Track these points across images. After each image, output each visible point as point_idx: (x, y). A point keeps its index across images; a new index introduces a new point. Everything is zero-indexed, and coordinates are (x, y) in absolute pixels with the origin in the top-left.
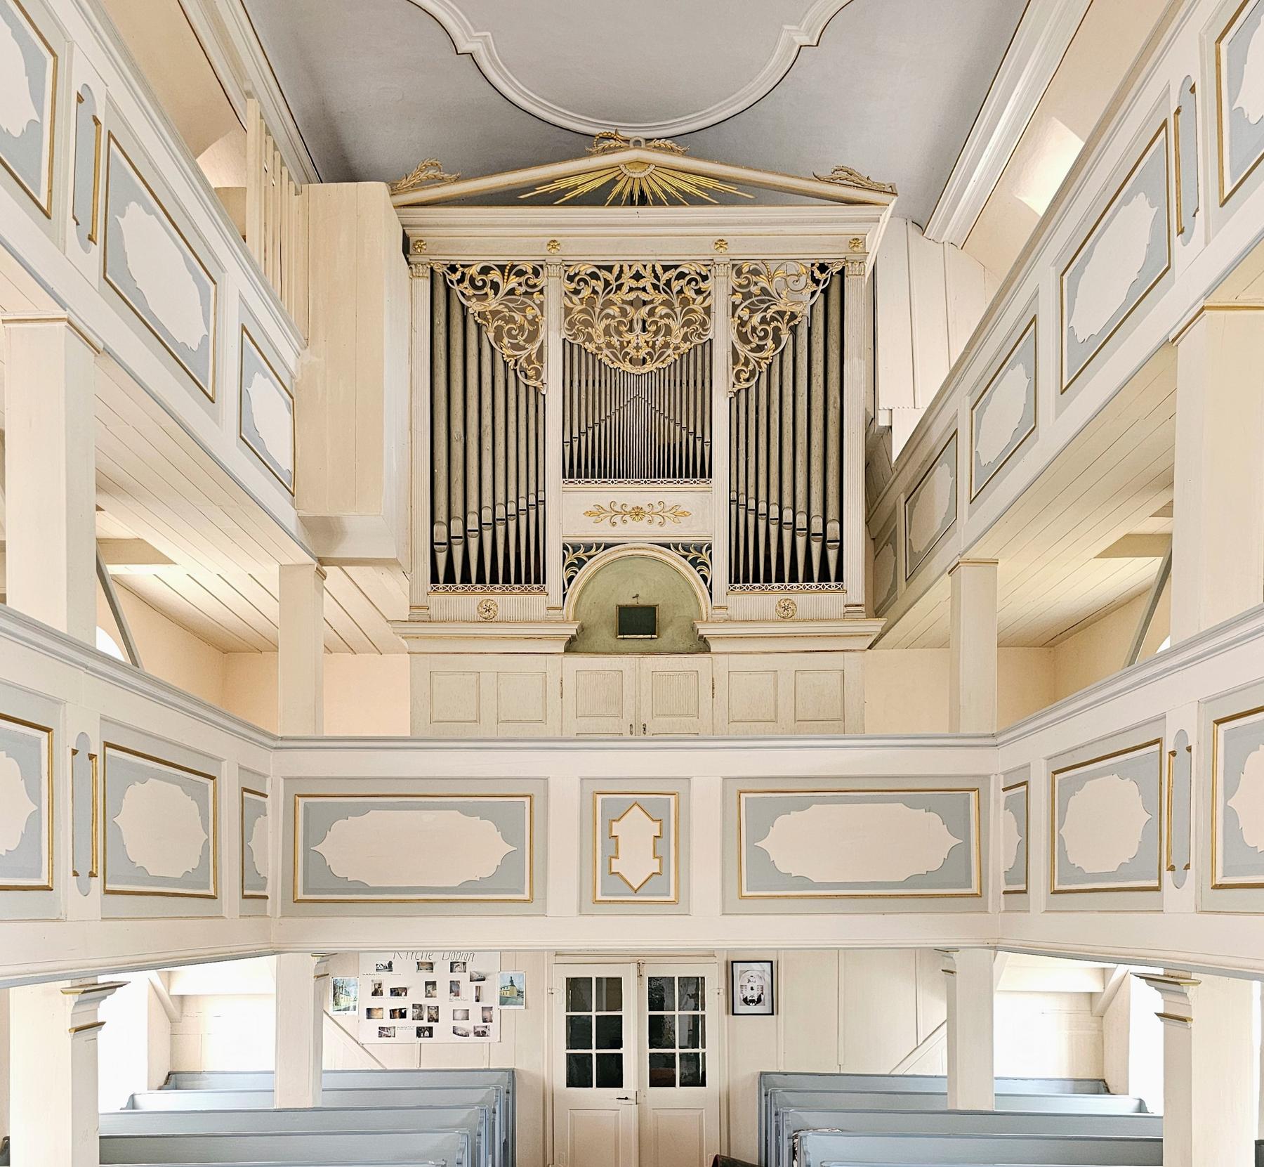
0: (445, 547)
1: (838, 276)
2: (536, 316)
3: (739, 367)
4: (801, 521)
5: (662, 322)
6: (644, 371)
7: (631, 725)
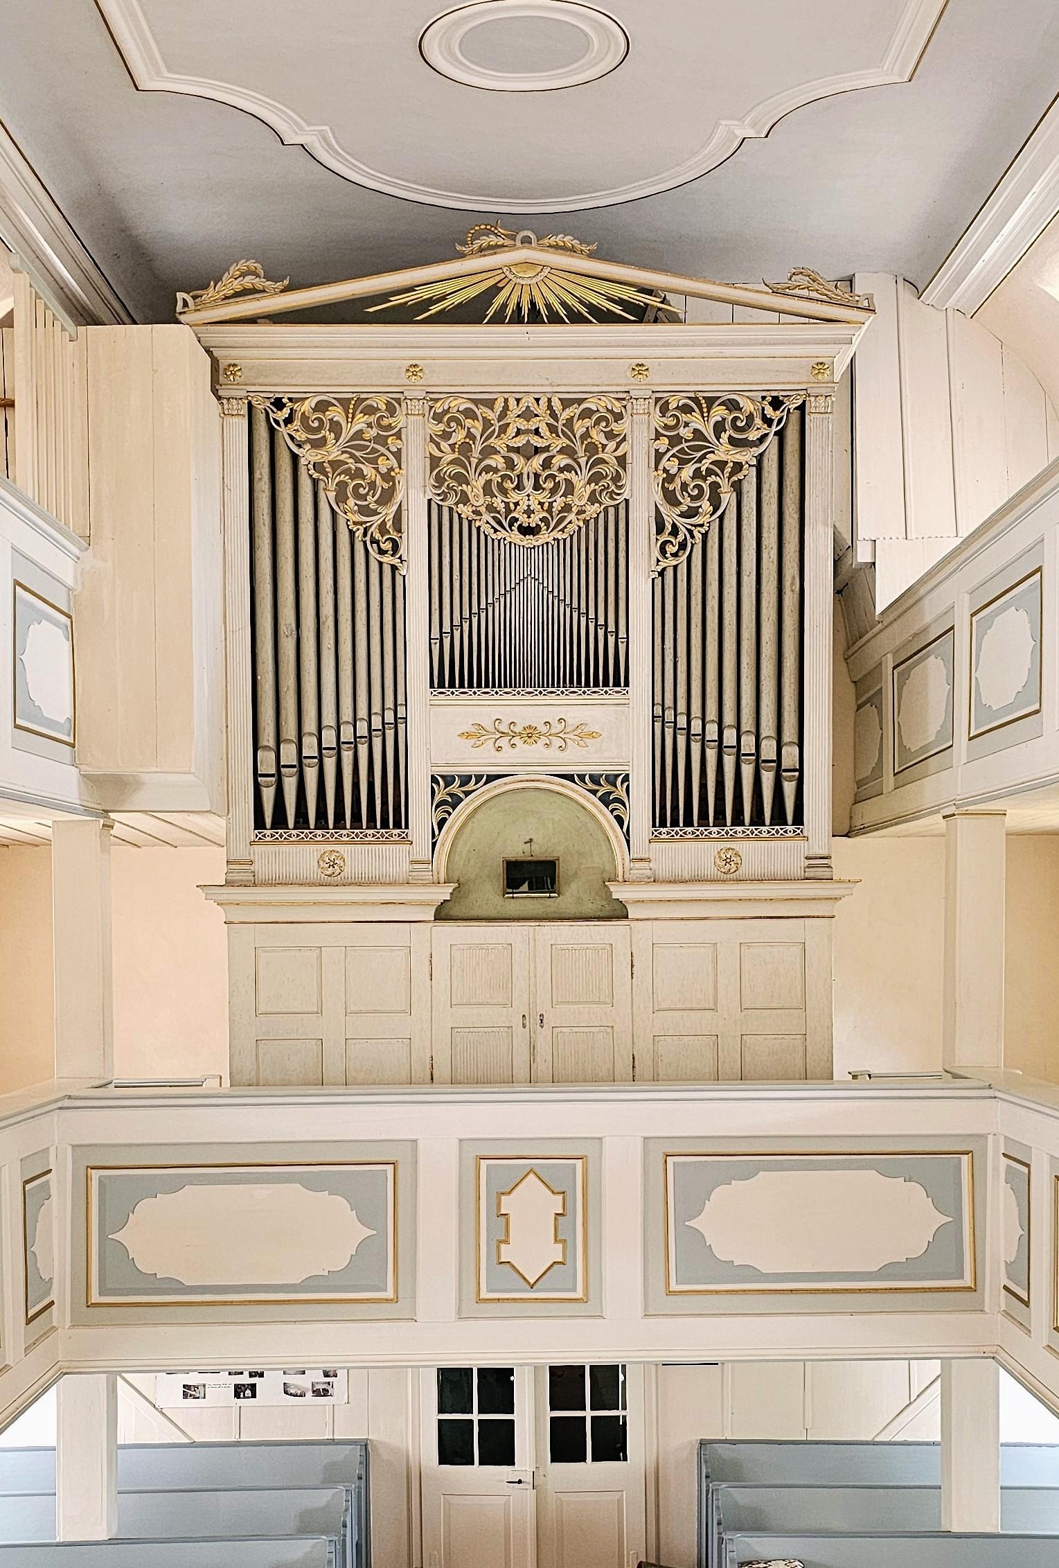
0: (273, 779)
1: (798, 412)
2: (392, 469)
3: (665, 537)
4: (748, 744)
5: (561, 477)
6: (536, 544)
7: (524, 1016)
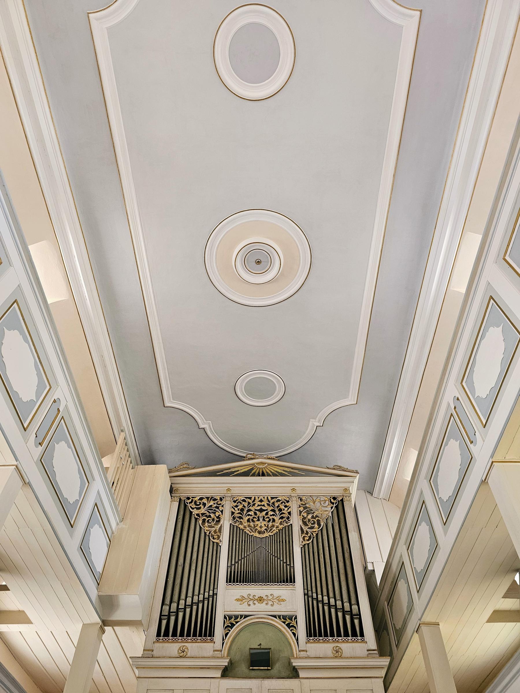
2: (220, 515)
5: (271, 517)
